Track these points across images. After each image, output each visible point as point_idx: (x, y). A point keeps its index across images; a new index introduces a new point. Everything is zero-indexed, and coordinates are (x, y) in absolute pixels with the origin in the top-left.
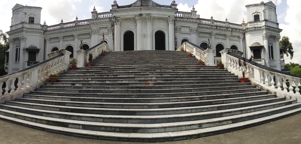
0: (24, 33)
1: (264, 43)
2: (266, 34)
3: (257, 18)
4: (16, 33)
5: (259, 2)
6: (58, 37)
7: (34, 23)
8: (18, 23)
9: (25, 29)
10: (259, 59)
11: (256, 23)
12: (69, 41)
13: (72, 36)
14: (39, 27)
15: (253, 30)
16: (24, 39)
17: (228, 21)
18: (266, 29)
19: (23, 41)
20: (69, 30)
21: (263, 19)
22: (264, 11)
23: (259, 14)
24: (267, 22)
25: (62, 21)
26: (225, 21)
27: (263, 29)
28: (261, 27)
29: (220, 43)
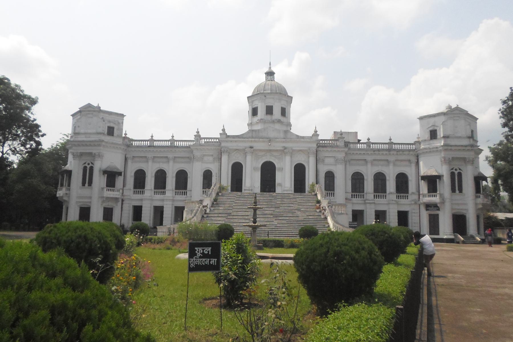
0: (101, 148)
1: (444, 171)
2: (444, 158)
3: (433, 135)
4: (86, 145)
5: (443, 109)
6: (146, 157)
7: (115, 135)
8: (89, 131)
9: (103, 143)
10: (435, 194)
11: (431, 142)
12: (161, 164)
13: (167, 157)
14: (120, 141)
15: (427, 152)
16: (100, 156)
17: (392, 141)
18: (446, 150)
19: (99, 159)
20: (162, 150)
21: (442, 136)
22: (443, 123)
23: (436, 128)
24: (449, 139)
25: (152, 137)
26: (388, 141)
27: (441, 150)
28: (437, 148)
29: (380, 171)
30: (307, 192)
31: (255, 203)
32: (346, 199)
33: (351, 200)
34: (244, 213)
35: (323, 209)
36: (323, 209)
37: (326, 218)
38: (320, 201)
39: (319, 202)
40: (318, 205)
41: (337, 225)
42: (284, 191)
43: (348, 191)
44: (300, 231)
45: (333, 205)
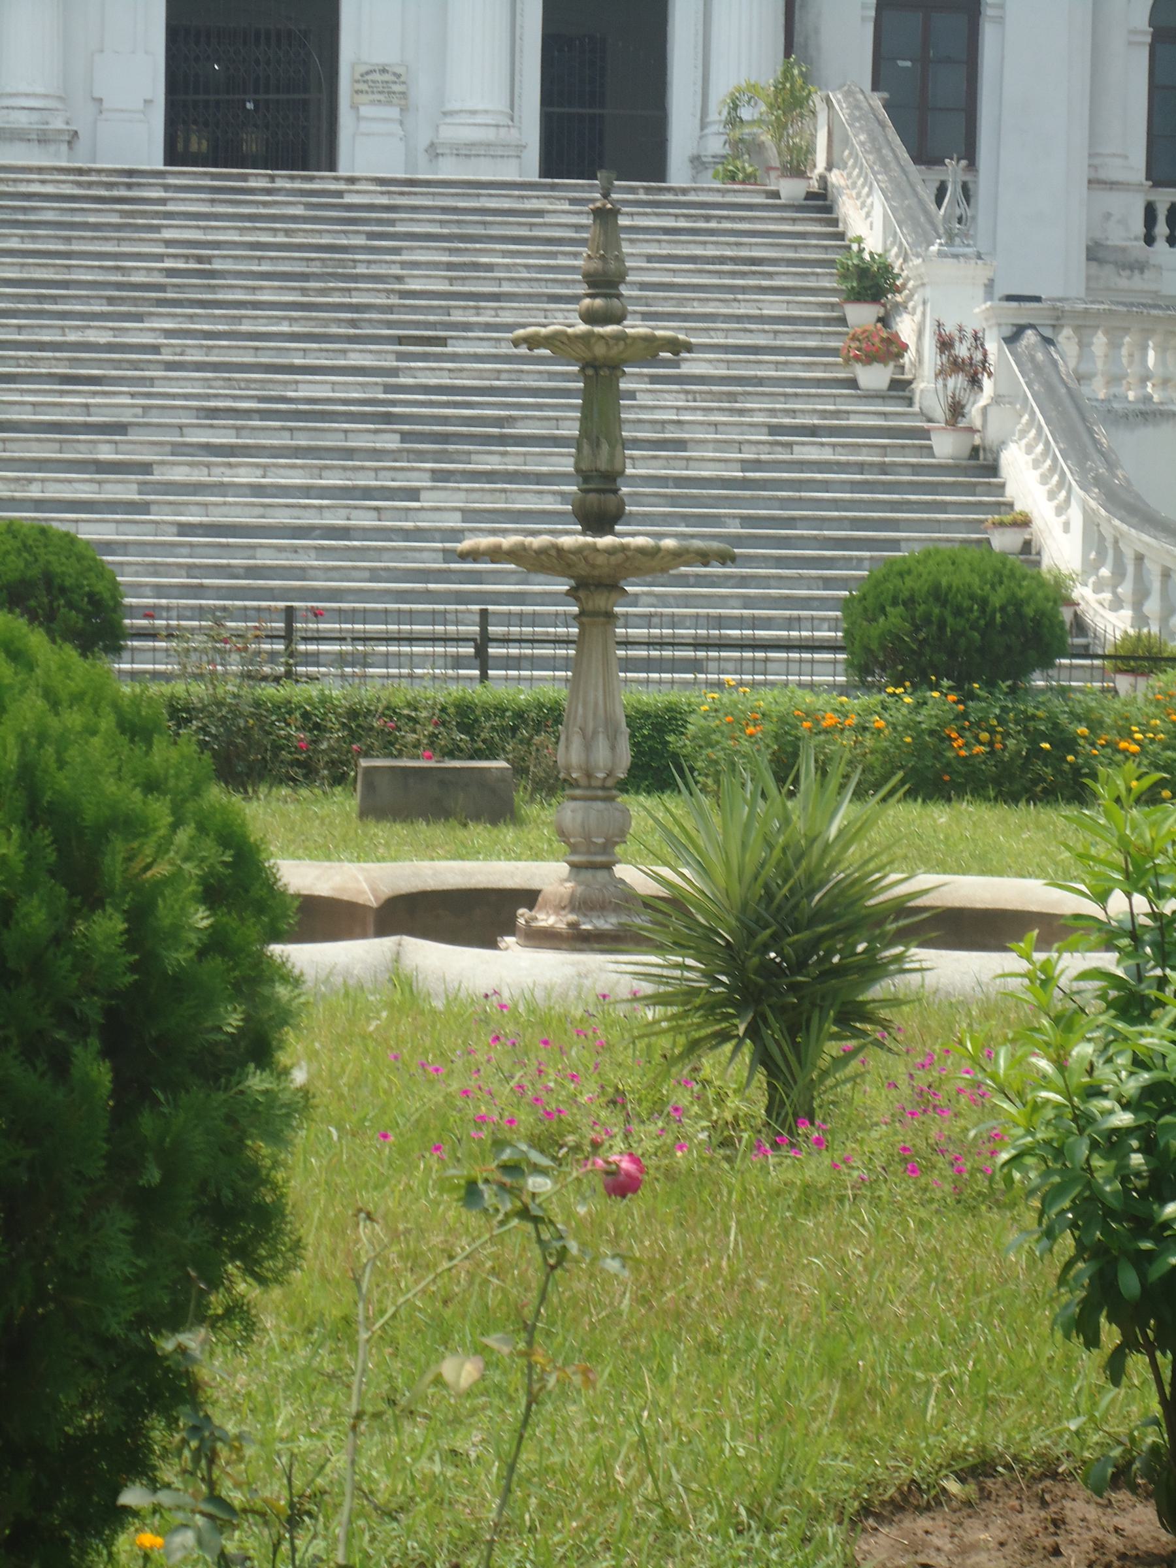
30: (678, 172)
31: (604, 282)
32: (1095, 253)
33: (1139, 267)
34: (71, 404)
35: (956, 365)
36: (956, 365)
37: (982, 464)
38: (886, 269)
39: (872, 283)
40: (861, 315)
41: (1138, 539)
42: (434, 152)
43: (1114, 172)
44: (866, 607)
45: (1058, 319)
